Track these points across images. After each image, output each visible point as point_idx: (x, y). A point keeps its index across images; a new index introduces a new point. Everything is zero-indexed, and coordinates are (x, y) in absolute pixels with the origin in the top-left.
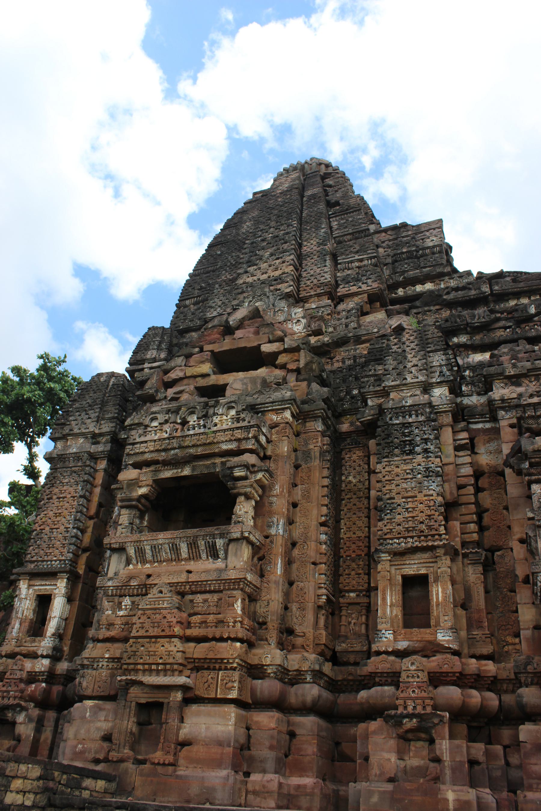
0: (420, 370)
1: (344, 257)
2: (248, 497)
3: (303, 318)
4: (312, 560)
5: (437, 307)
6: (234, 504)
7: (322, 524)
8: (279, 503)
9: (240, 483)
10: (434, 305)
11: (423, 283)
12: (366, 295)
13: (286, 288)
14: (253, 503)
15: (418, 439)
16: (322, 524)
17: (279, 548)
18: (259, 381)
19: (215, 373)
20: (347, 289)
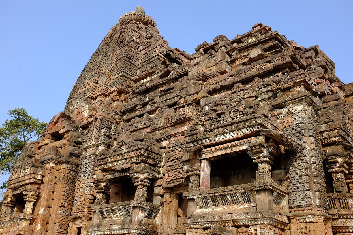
0: (95, 139)
1: (114, 73)
2: (30, 201)
3: (88, 109)
4: (53, 222)
5: (136, 95)
6: (25, 204)
7: (60, 207)
8: (43, 201)
9: (26, 197)
10: (135, 94)
11: (146, 78)
12: (116, 92)
13: (88, 94)
14: (33, 203)
15: (88, 170)
16: (60, 207)
17: (39, 219)
18: (51, 148)
19: (51, 142)
20: (110, 90)
